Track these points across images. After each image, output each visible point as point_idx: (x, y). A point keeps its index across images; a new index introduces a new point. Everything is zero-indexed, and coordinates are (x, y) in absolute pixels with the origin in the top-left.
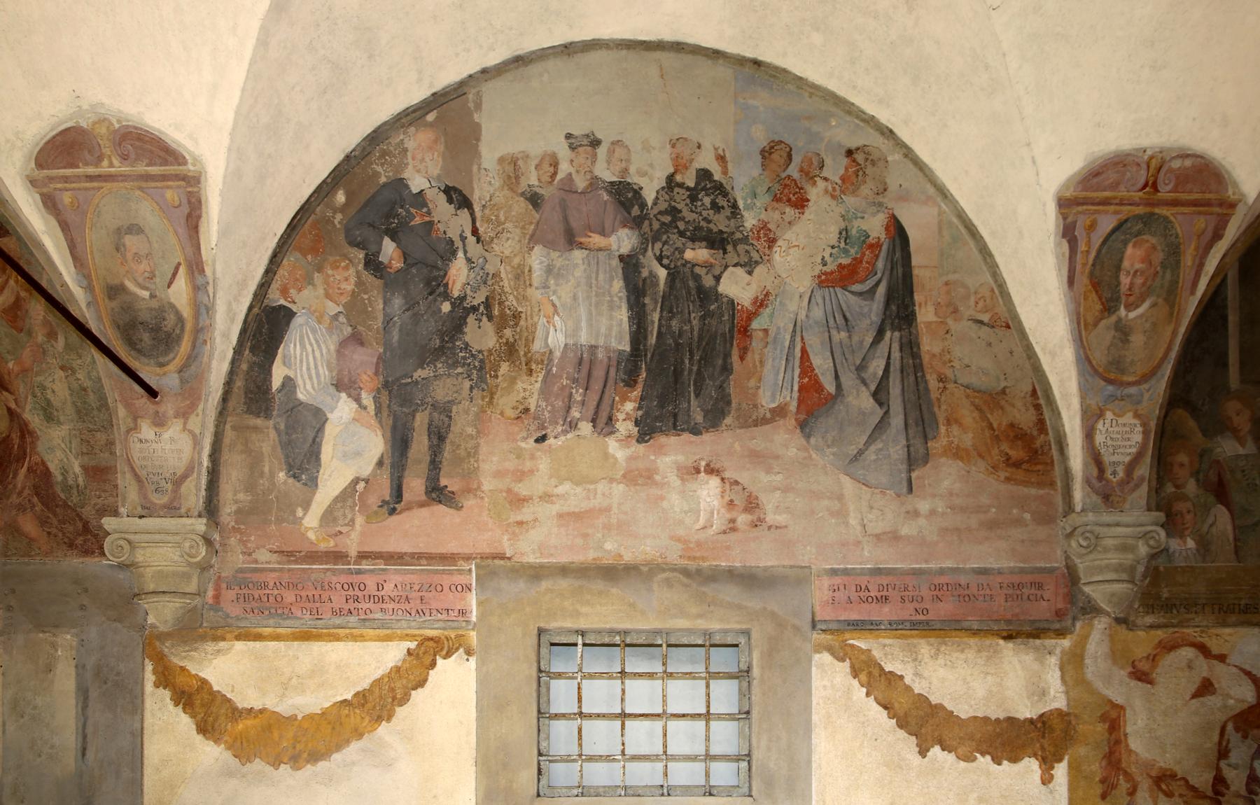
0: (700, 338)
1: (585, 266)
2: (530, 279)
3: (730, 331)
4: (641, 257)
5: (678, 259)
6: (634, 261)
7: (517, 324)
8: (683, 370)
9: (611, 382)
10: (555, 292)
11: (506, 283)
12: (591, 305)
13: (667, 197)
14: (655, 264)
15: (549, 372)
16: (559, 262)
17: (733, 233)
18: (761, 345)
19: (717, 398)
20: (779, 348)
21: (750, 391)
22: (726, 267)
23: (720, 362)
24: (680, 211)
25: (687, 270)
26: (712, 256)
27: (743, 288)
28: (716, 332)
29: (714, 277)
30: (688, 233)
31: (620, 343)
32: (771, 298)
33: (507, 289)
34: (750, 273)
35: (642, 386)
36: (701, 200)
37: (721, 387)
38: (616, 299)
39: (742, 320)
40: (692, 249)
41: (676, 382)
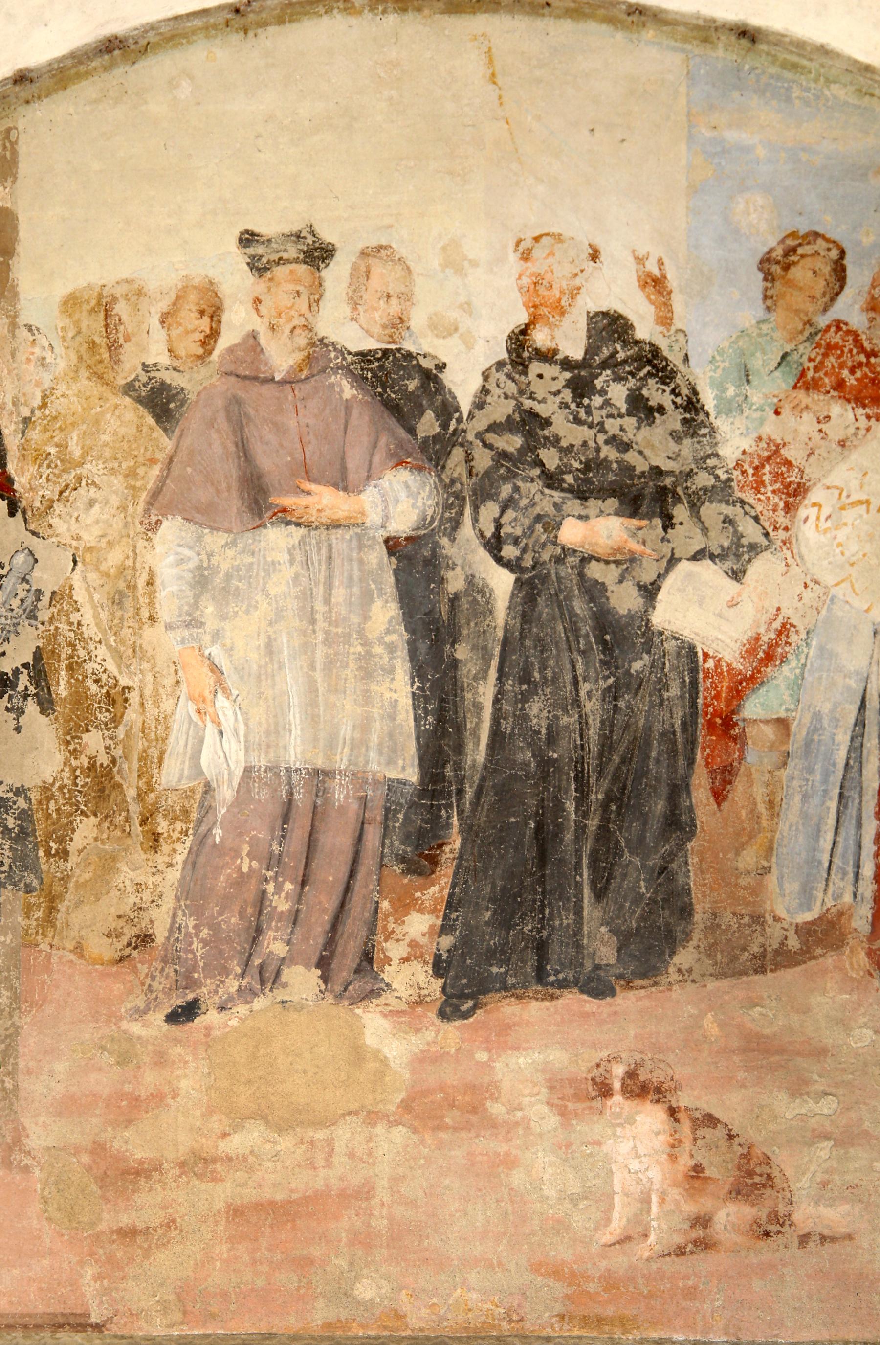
0: (607, 745)
1: (297, 568)
2: (151, 604)
3: (684, 724)
4: (445, 541)
5: (544, 545)
6: (427, 553)
7: (116, 721)
8: (560, 829)
9: (368, 863)
10: (216, 636)
11: (87, 616)
12: (312, 667)
13: (511, 388)
14: (483, 556)
15: (202, 841)
16: (226, 561)
17: (690, 474)
18: (770, 760)
19: (653, 901)
20: (818, 767)
21: (743, 882)
22: (673, 561)
23: (659, 806)
24: (547, 423)
25: (566, 570)
26: (634, 535)
27: (720, 615)
28: (648, 729)
29: (641, 587)
30: (569, 479)
31: (390, 762)
32: (793, 638)
33: (91, 631)
34: (737, 575)
35: (450, 872)
36: (603, 392)
37: (663, 870)
38: (378, 650)
39: (717, 697)
40: (580, 517)
41: (542, 858)
